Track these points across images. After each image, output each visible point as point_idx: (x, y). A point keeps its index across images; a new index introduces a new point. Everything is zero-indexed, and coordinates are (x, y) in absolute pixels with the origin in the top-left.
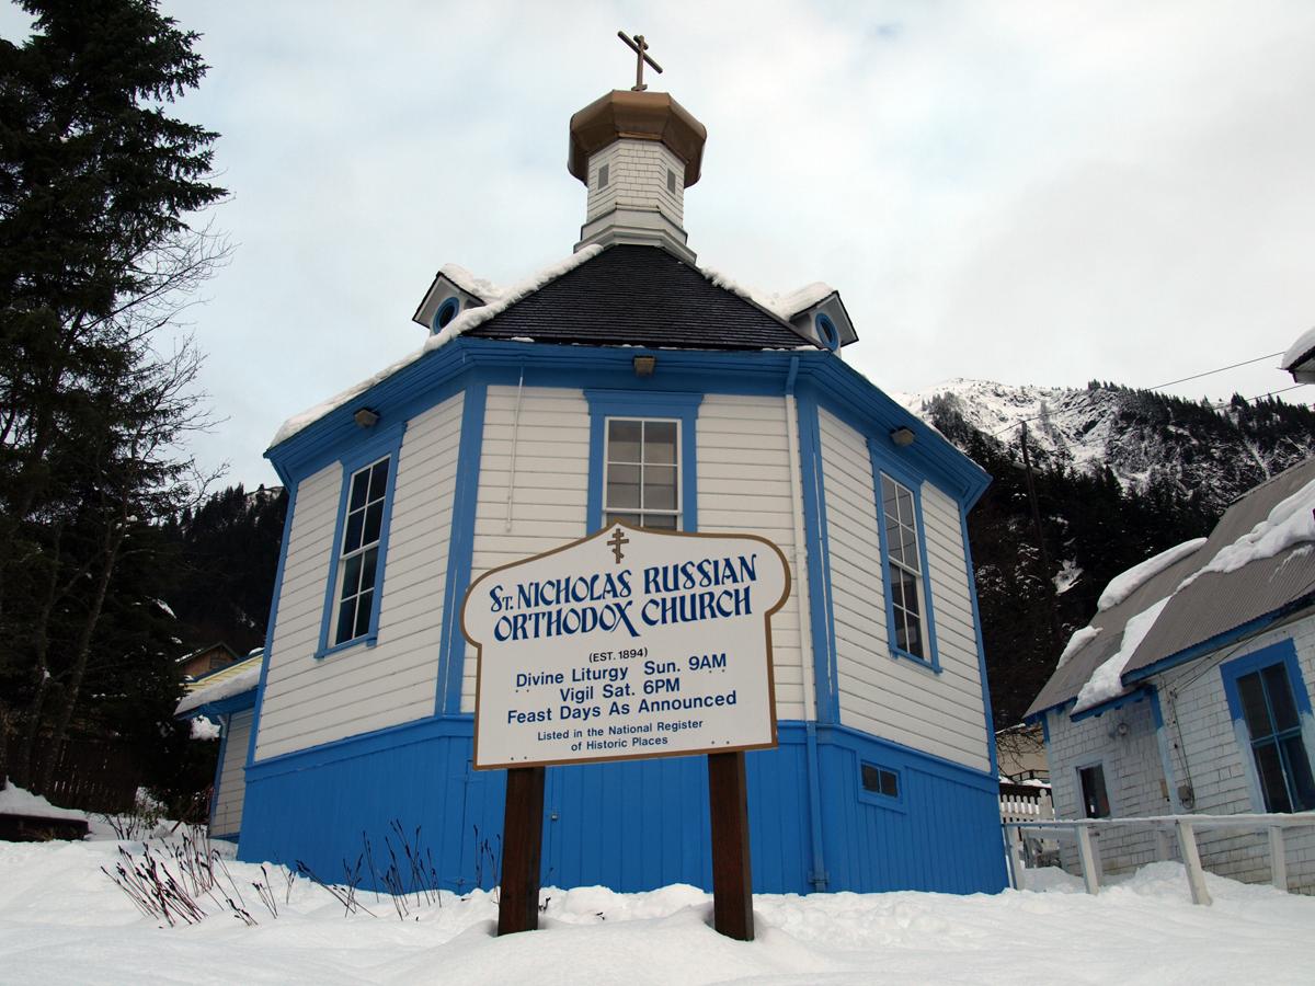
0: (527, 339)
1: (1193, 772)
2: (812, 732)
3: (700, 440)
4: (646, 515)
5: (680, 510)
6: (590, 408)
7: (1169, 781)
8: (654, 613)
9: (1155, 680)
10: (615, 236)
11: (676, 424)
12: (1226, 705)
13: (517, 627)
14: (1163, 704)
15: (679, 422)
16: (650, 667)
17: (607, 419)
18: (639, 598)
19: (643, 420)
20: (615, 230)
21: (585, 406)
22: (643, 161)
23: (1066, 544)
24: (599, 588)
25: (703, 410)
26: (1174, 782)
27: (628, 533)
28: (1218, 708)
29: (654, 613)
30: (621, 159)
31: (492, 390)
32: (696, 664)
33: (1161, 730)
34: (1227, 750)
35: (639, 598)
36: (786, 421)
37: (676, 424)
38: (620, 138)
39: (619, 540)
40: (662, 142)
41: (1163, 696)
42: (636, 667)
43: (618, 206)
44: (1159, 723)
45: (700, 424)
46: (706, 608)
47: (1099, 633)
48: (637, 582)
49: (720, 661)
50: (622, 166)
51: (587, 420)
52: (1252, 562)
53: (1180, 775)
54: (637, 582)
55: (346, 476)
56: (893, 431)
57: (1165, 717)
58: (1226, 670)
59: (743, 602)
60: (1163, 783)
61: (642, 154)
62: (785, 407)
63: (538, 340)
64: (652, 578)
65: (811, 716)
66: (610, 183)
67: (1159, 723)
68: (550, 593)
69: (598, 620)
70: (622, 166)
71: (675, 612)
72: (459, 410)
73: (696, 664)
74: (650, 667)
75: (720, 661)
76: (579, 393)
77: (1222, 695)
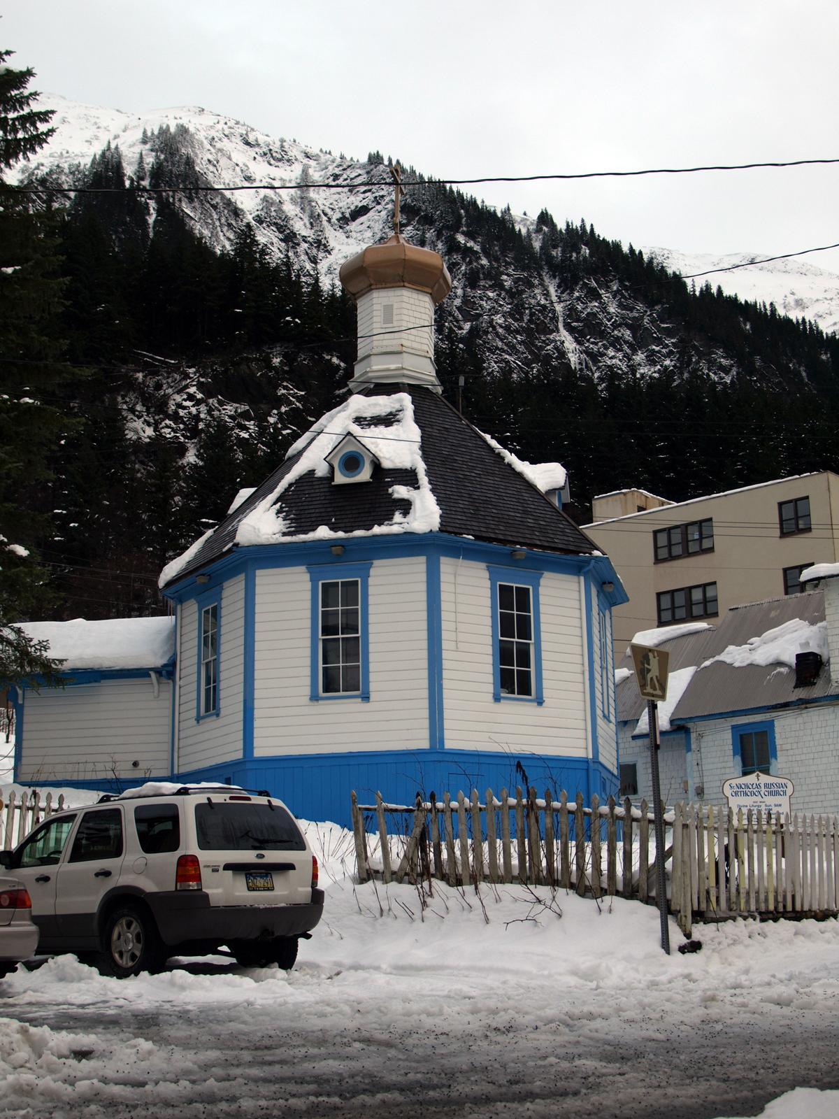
0: (471, 537)
1: (705, 779)
2: (591, 764)
5: (533, 641)
7: (690, 782)
8: (766, 793)
9: (690, 725)
10: (404, 376)
11: (528, 589)
12: (731, 747)
13: (736, 793)
14: (693, 740)
15: (531, 588)
16: (766, 805)
18: (763, 790)
20: (405, 372)
21: (487, 575)
22: (418, 309)
23: (337, 392)
24: (754, 786)
26: (693, 783)
27: (760, 774)
28: (727, 748)
29: (766, 793)
30: (404, 305)
32: (776, 805)
33: (689, 753)
34: (728, 770)
35: (763, 790)
36: (579, 591)
37: (528, 589)
38: (404, 286)
39: (758, 776)
40: (431, 294)
41: (693, 736)
42: (763, 805)
43: (404, 349)
44: (689, 749)
45: (541, 590)
46: (777, 793)
47: (632, 674)
48: (762, 786)
49: (780, 805)
50: (405, 312)
51: (488, 583)
52: (751, 665)
53: (697, 780)
54: (762, 786)
55: (314, 581)
56: (604, 583)
57: (693, 746)
58: (733, 727)
59: (785, 793)
60: (686, 783)
61: (417, 302)
62: (579, 583)
63: (477, 538)
64: (766, 785)
65: (591, 756)
66: (395, 324)
67: (689, 749)
68: (743, 786)
69: (754, 794)
70: (405, 312)
71: (771, 794)
72: (423, 567)
73: (776, 805)
74: (766, 805)
75: (780, 805)
76: (483, 565)
77: (730, 741)
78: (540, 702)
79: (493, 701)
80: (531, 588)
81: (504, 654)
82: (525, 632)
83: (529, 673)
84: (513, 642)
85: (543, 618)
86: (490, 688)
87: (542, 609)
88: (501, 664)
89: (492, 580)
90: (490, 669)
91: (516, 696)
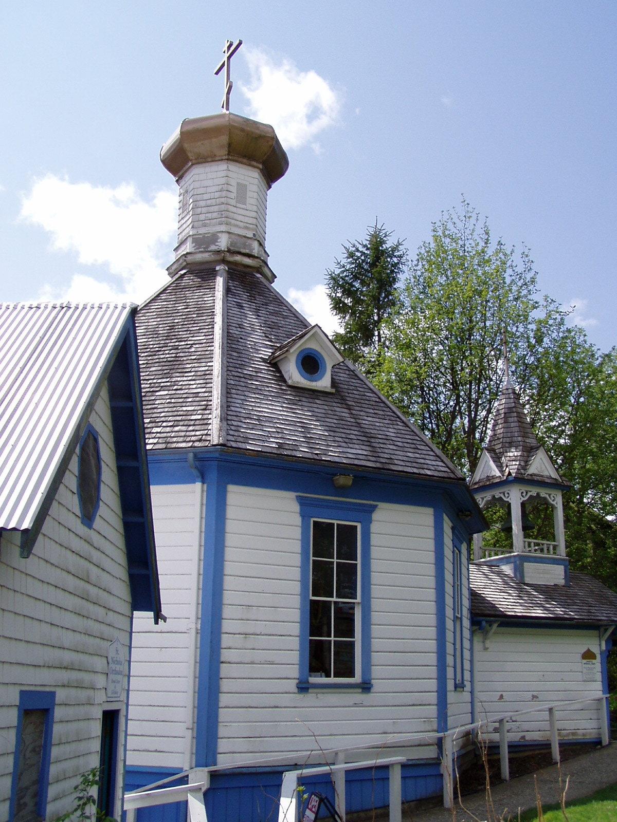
3: (374, 539)
4: (335, 602)
5: (359, 600)
6: (301, 510)
11: (356, 527)
15: (359, 526)
17: (312, 520)
19: (335, 522)
21: (296, 507)
25: (376, 516)
31: (231, 488)
37: (356, 527)
45: (374, 527)
51: (298, 520)
78: (366, 687)
79: (296, 690)
80: (359, 526)
81: (317, 617)
82: (348, 585)
83: (352, 645)
84: (330, 602)
85: (375, 565)
86: (294, 672)
87: (375, 552)
88: (310, 636)
89: (304, 516)
90: (295, 643)
91: (332, 680)
